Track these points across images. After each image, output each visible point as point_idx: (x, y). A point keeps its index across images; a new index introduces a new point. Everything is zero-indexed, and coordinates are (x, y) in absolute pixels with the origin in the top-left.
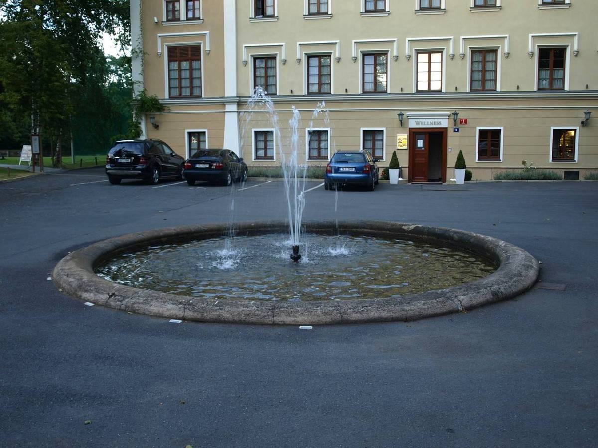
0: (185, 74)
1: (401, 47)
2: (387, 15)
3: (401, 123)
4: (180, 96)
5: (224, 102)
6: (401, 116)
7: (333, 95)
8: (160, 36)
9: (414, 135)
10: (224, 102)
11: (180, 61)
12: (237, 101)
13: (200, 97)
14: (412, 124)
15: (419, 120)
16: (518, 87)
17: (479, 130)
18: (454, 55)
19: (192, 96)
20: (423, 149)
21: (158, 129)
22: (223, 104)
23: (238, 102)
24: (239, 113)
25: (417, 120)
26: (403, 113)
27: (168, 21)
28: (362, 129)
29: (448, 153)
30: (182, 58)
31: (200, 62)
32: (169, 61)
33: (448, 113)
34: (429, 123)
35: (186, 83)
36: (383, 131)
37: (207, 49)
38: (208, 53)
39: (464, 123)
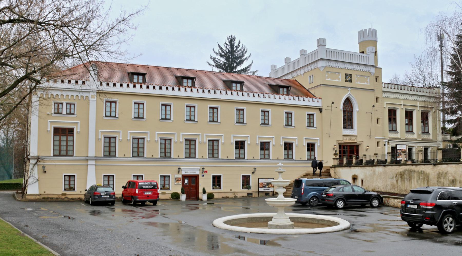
0: (64, 143)
1: (178, 137)
4: (60, 155)
5: (87, 159)
7: (118, 157)
8: (50, 121)
9: (184, 177)
10: (87, 159)
11: (60, 136)
13: (72, 156)
14: (183, 173)
17: (213, 176)
19: (67, 155)
20: (188, 184)
21: (46, 172)
22: (87, 160)
24: (95, 165)
27: (55, 113)
32: (54, 135)
33: (199, 168)
35: (64, 148)
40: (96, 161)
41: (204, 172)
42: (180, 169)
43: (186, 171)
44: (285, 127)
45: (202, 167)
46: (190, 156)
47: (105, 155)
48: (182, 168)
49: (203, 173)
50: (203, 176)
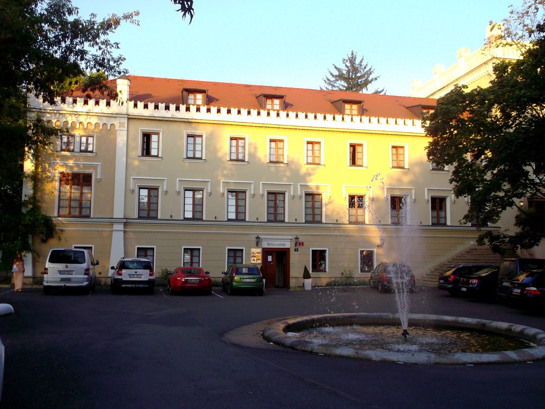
1: (256, 188)
2: (247, 164)
3: (257, 243)
6: (258, 239)
9: (266, 252)
10: (112, 221)
12: (125, 222)
13: (88, 217)
14: (265, 245)
15: (270, 242)
16: (171, 216)
17: (312, 250)
18: (294, 196)
22: (112, 224)
23: (124, 223)
24: (125, 232)
25: (268, 242)
26: (259, 236)
28: (227, 248)
29: (290, 266)
30: (84, 184)
31: (90, 187)
33: (290, 237)
34: (277, 244)
36: (242, 250)
37: (98, 177)
38: (99, 181)
39: (301, 245)
40: (125, 224)
41: (298, 244)
42: (259, 238)
43: (270, 242)
44: (431, 172)
45: (295, 237)
46: (275, 219)
47: (141, 215)
48: (262, 237)
49: (296, 245)
50: (296, 250)
